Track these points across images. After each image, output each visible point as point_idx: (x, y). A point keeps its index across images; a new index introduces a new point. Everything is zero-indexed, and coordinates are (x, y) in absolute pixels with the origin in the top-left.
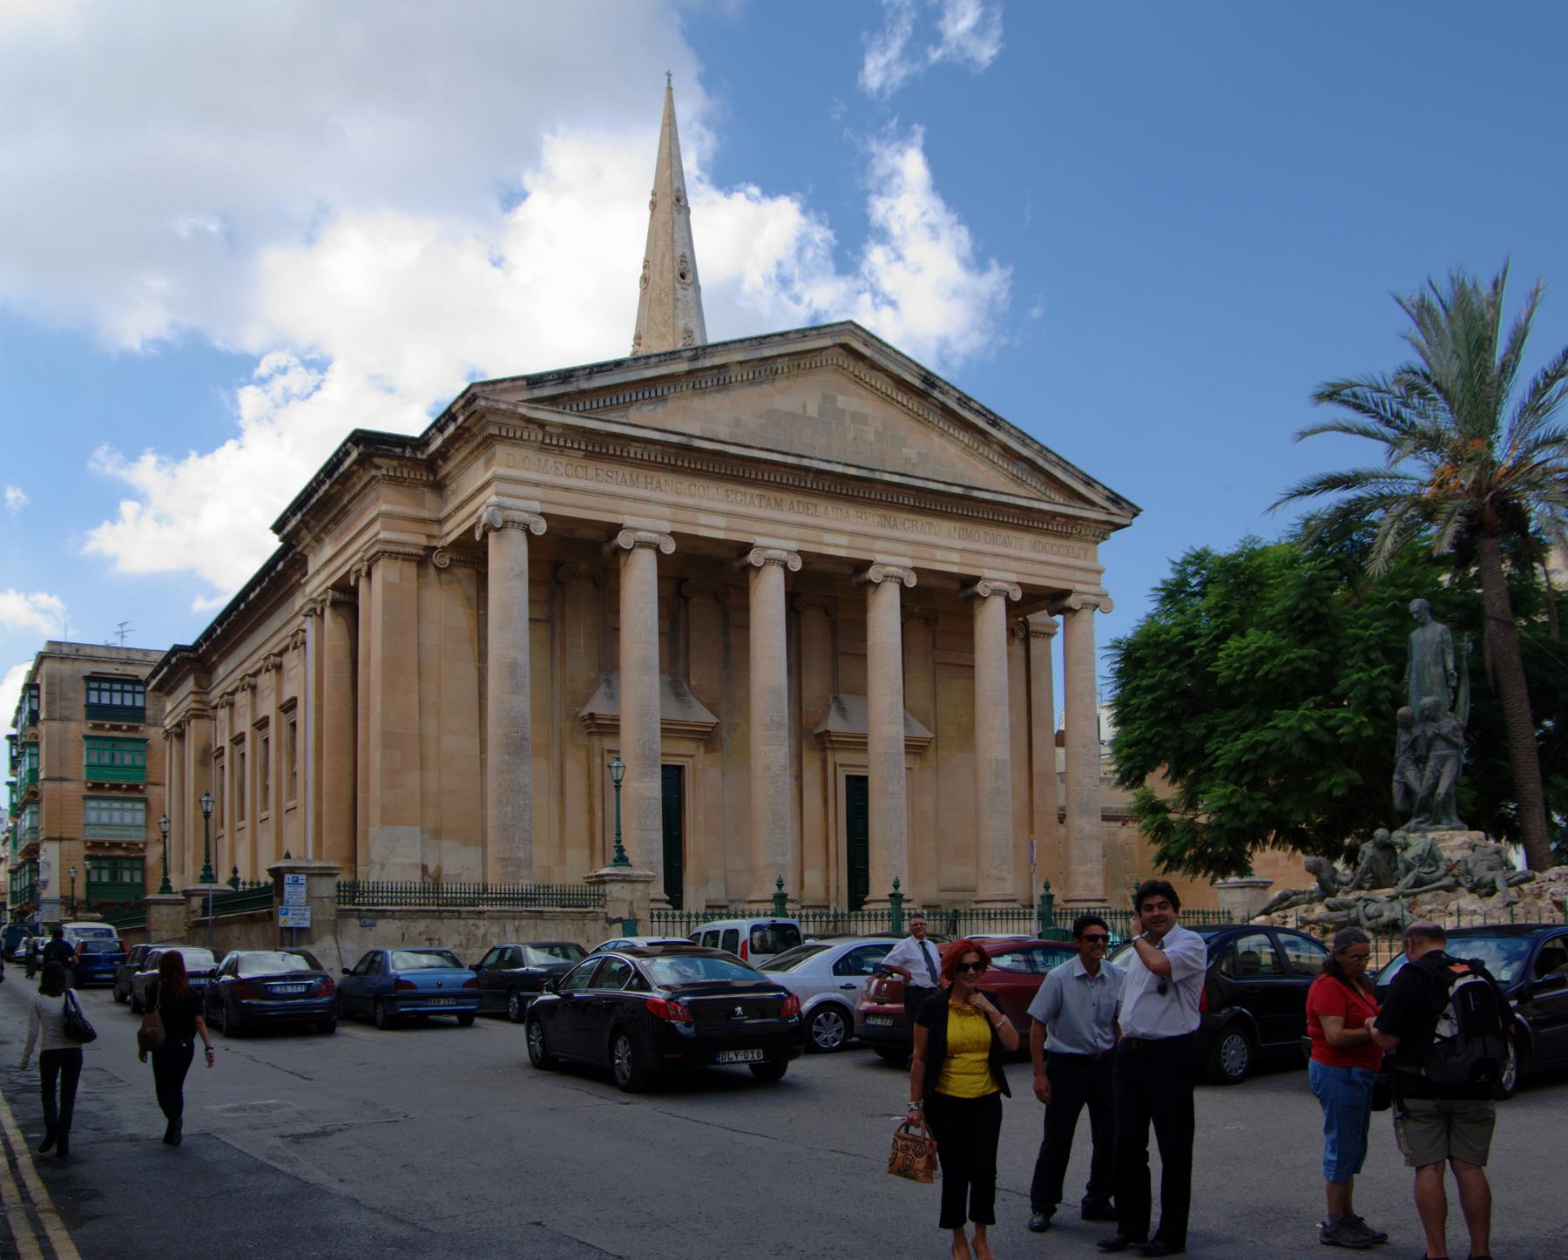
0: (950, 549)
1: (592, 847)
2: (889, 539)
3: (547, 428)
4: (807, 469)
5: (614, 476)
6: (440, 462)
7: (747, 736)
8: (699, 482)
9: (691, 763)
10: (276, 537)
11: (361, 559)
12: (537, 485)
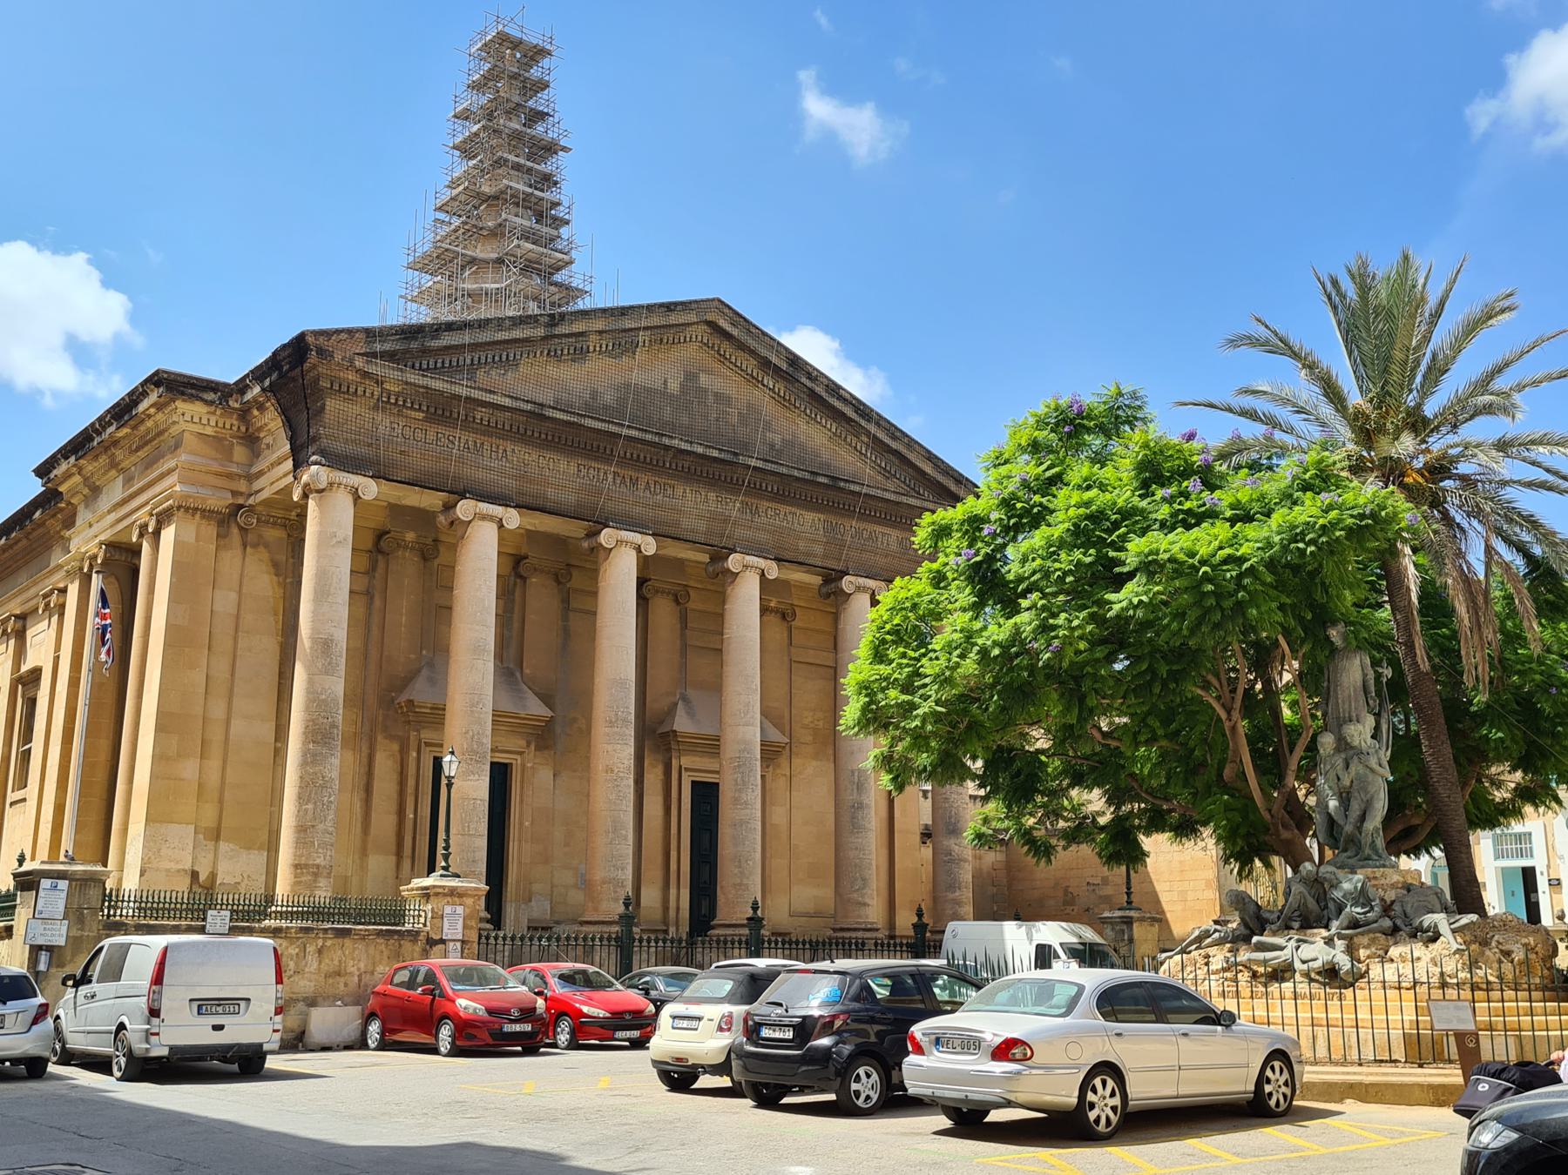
4: (667, 448)
6: (256, 412)
7: (587, 731)
9: (519, 762)
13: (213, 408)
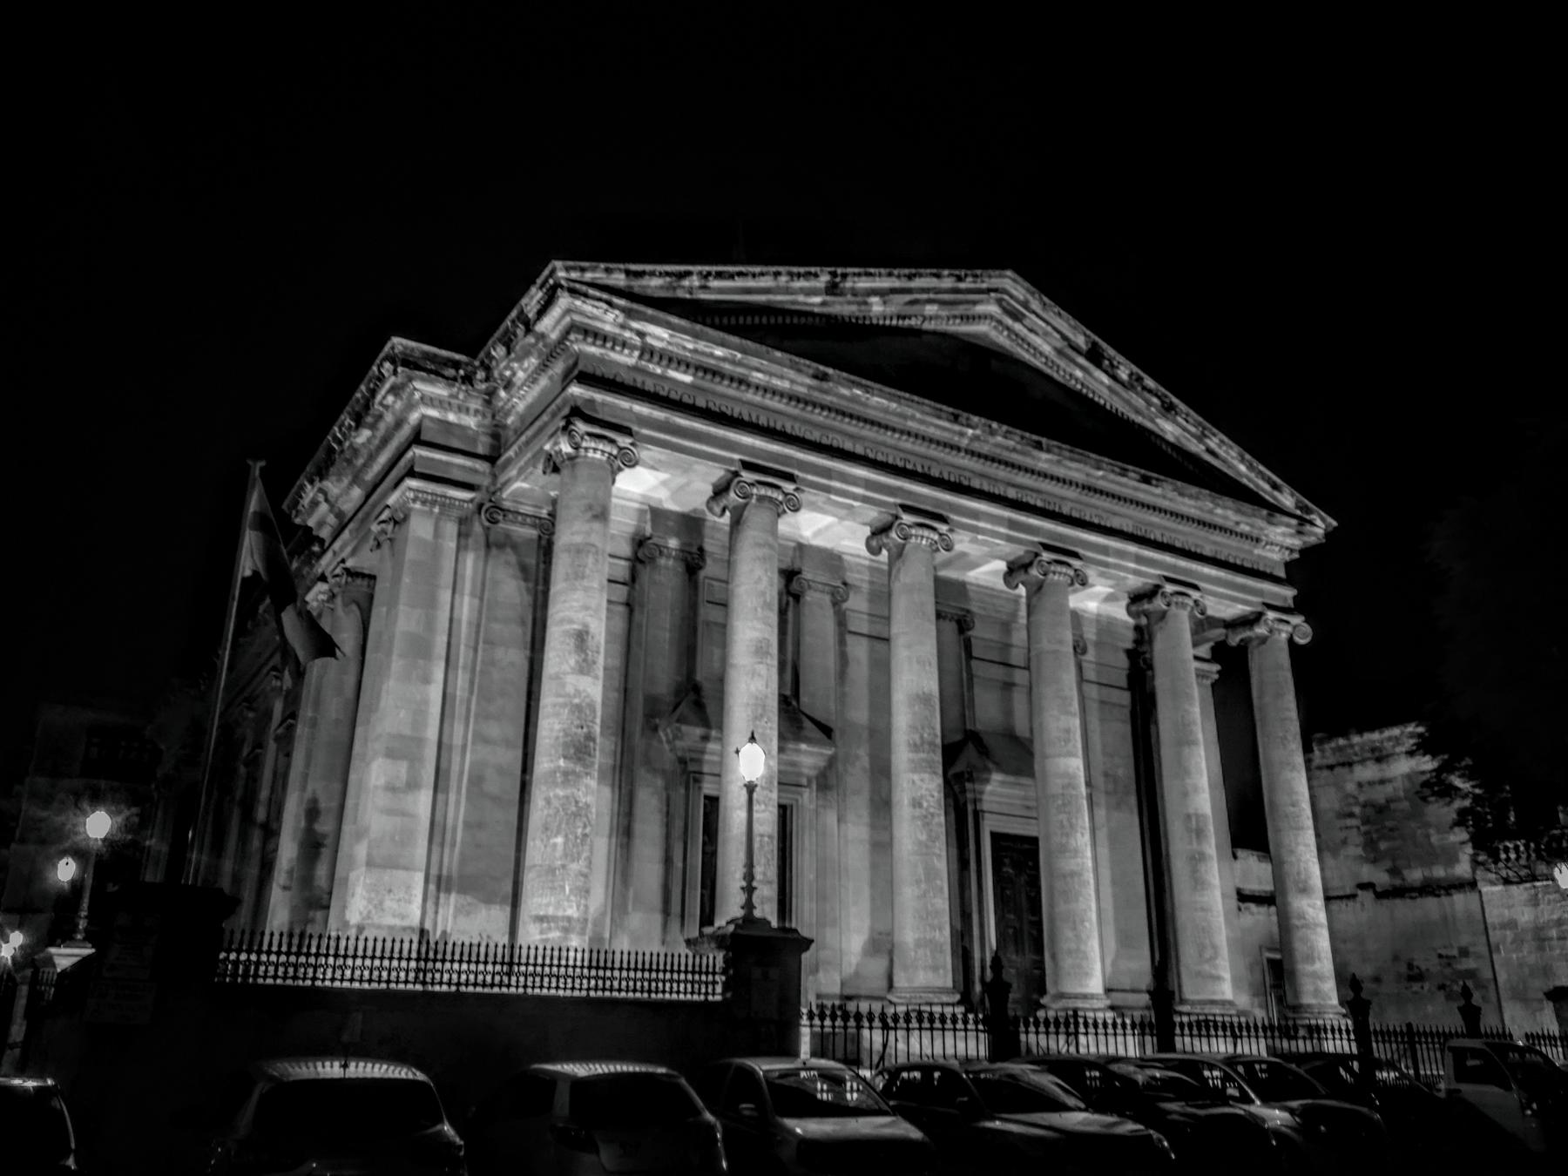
1: (666, 912)
6: (502, 394)
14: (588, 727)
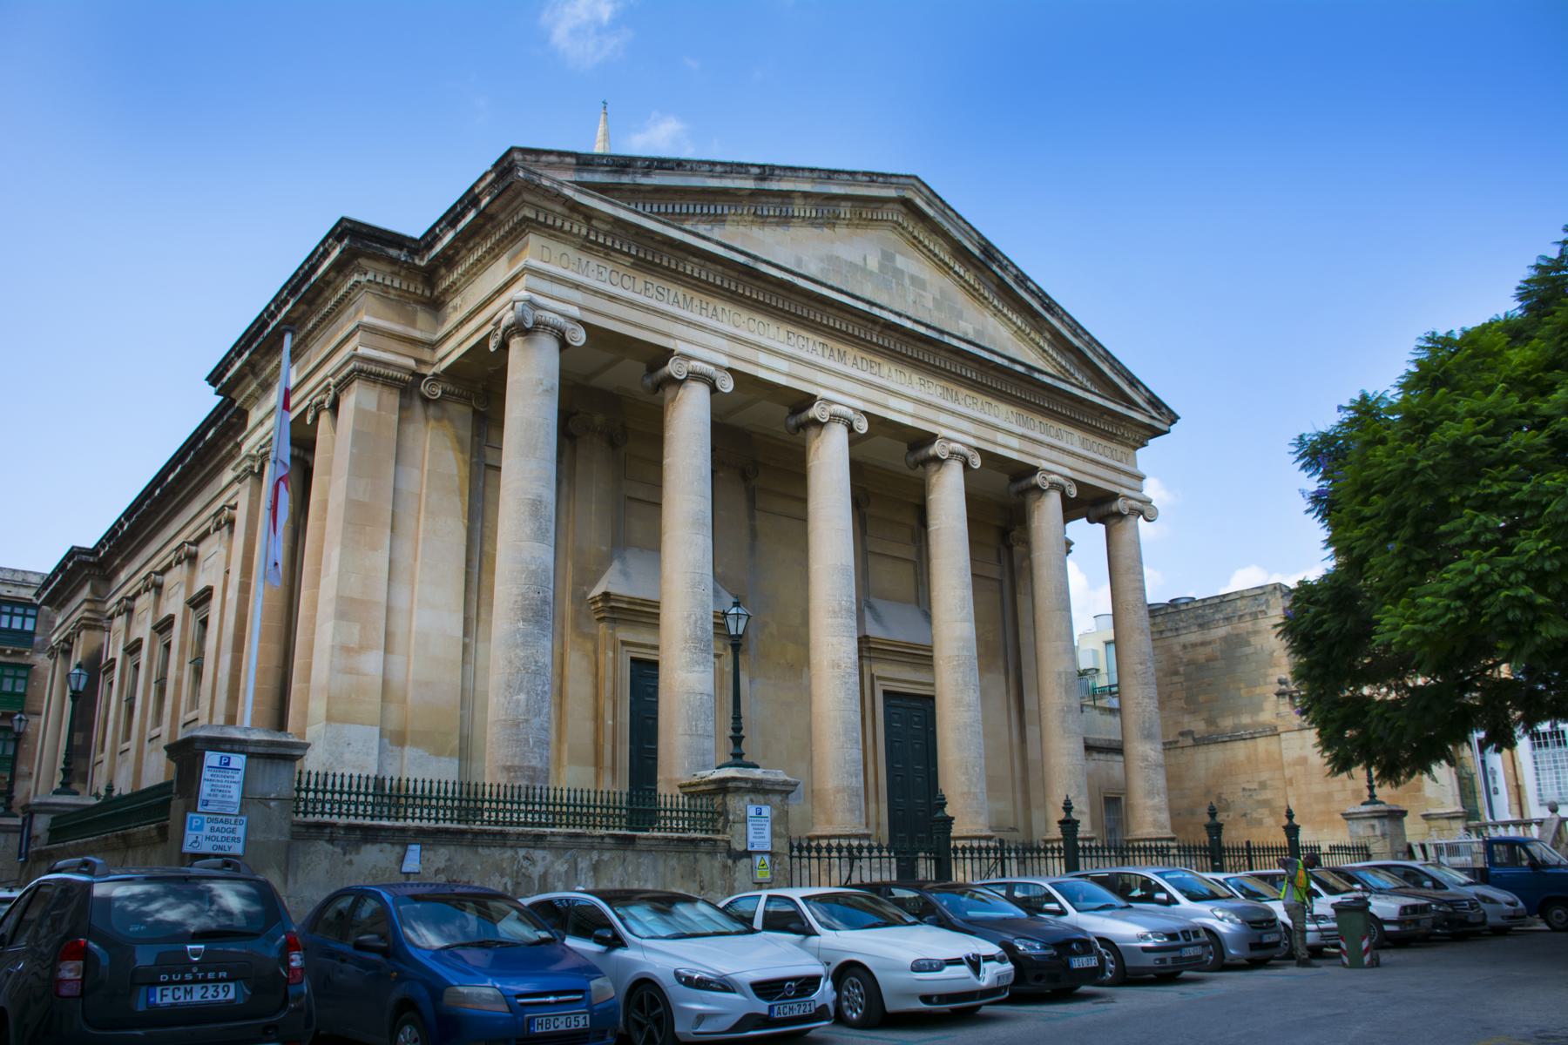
0: (1010, 433)
2: (953, 413)
3: (595, 223)
4: (875, 320)
5: (666, 293)
8: (758, 318)
10: (213, 389)
11: (327, 389)
12: (577, 286)
13: (396, 269)
14: (544, 591)
